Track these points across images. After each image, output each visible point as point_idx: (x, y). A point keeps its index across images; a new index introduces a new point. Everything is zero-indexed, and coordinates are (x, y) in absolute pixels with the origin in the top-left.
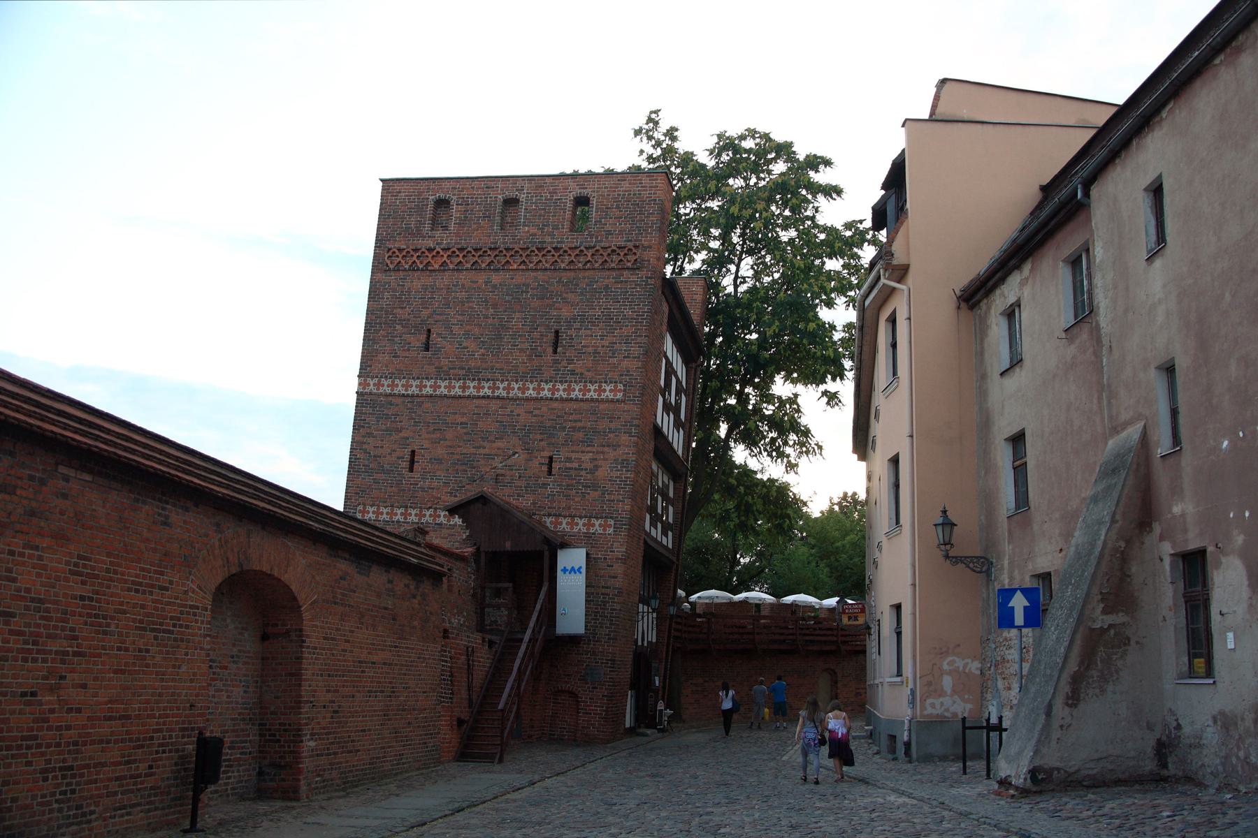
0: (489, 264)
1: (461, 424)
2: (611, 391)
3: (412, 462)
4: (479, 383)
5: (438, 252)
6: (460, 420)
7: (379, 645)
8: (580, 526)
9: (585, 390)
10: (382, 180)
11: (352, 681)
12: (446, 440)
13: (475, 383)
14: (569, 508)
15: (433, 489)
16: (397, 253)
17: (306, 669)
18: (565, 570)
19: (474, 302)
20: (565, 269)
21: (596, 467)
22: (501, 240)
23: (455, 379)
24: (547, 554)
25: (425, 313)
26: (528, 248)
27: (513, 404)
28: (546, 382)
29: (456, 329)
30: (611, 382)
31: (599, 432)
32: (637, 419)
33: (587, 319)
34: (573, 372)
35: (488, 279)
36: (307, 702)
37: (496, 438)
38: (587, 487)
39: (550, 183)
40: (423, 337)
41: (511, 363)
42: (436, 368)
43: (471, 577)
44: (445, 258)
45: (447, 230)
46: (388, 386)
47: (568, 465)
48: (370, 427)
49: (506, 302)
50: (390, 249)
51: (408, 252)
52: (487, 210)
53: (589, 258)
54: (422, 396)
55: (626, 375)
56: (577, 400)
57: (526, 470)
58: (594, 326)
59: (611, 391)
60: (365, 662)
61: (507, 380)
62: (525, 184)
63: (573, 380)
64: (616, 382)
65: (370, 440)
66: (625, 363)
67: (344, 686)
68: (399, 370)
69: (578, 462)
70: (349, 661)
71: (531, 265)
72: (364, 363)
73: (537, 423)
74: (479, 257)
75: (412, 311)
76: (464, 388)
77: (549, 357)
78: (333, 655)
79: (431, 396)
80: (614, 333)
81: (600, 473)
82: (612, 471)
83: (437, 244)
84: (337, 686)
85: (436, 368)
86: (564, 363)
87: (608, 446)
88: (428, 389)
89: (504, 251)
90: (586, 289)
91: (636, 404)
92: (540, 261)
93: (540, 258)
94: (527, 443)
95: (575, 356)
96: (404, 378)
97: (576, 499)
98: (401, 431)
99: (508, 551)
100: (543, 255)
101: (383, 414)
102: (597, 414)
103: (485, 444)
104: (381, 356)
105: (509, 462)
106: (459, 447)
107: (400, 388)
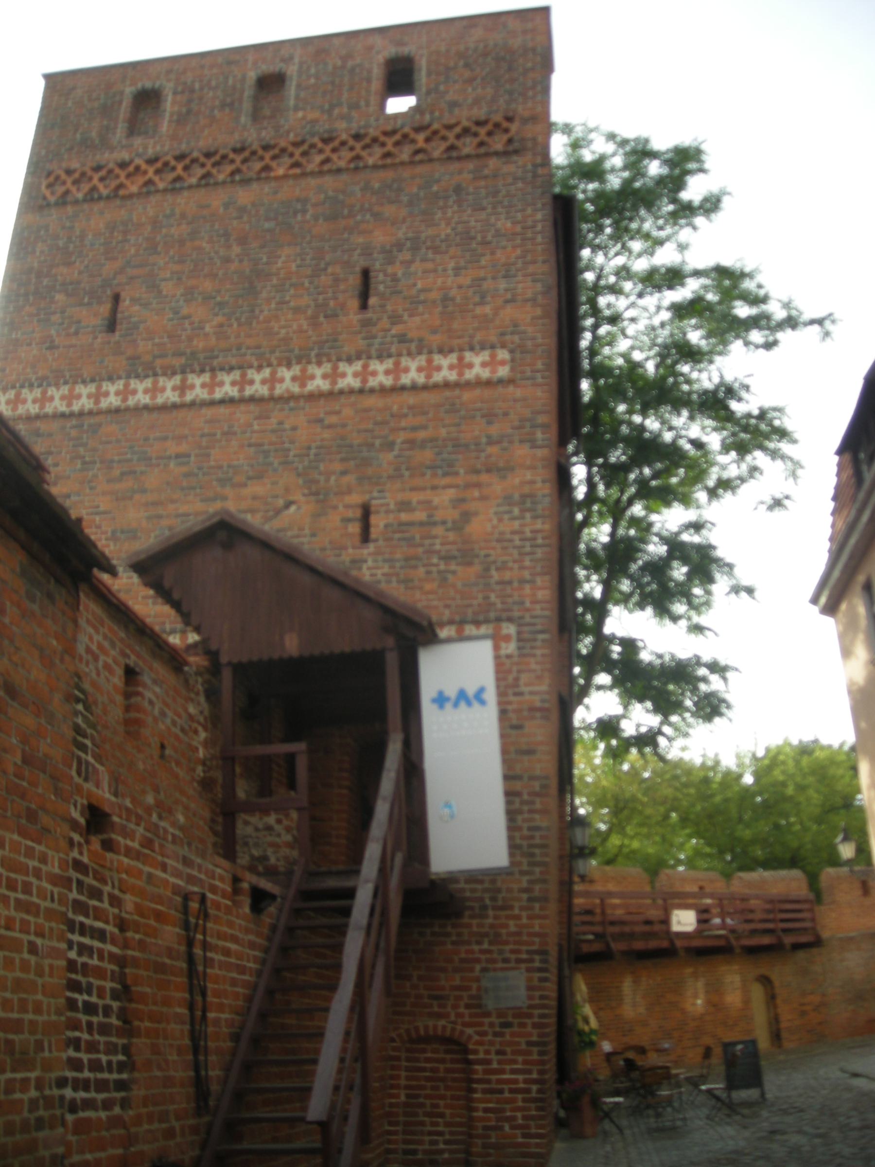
0: (233, 174)
1: (178, 456)
4: (213, 377)
6: (172, 448)
9: (430, 368)
13: (206, 377)
21: (467, 516)
22: (253, 136)
23: (164, 374)
24: (392, 661)
26: (303, 142)
27: (282, 410)
28: (349, 360)
29: (167, 288)
30: (483, 348)
31: (466, 446)
33: (424, 243)
34: (402, 339)
37: (249, 478)
38: (447, 558)
40: (105, 309)
42: (128, 359)
43: (196, 732)
47: (404, 517)
54: (100, 412)
55: (512, 333)
56: (414, 388)
57: (313, 535)
61: (269, 365)
64: (493, 347)
66: (509, 312)
75: (87, 267)
76: (183, 388)
77: (354, 317)
79: (117, 411)
80: (478, 261)
81: (476, 527)
82: (500, 520)
85: (128, 359)
86: (385, 322)
87: (489, 471)
95: (404, 310)
96: (66, 383)
97: (428, 587)
100: (334, 150)
103: (228, 491)
106: (173, 501)
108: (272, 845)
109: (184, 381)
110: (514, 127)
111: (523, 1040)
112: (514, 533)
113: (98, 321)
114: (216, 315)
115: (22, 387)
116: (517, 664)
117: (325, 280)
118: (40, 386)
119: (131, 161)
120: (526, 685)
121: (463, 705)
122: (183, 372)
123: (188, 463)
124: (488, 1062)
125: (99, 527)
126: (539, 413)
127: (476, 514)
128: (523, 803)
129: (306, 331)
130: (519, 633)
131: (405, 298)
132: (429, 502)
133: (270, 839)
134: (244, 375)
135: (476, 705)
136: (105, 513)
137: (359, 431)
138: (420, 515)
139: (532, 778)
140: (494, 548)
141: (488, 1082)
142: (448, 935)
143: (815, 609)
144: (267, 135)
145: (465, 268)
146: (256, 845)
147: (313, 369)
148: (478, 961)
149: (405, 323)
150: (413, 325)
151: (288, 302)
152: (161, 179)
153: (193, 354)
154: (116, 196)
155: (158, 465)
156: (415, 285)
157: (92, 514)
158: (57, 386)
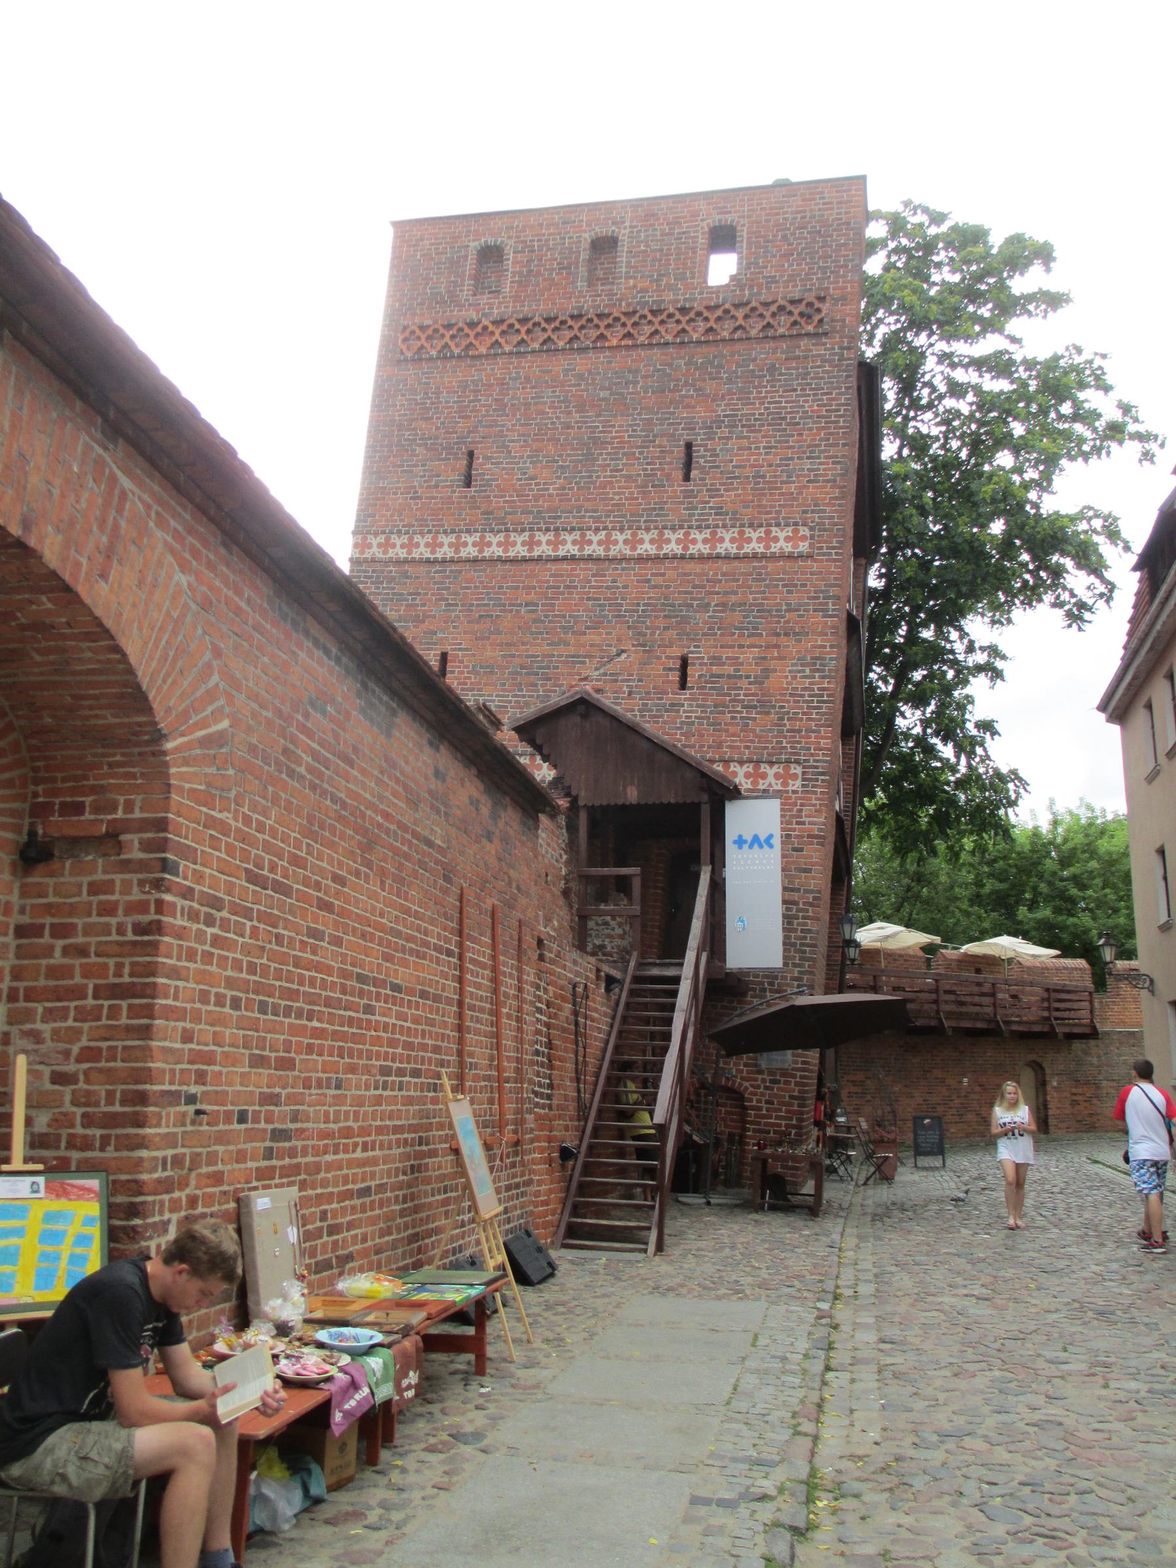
0: (571, 341)
4: (557, 535)
5: (485, 328)
7: (409, 939)
9: (742, 540)
11: (336, 1036)
12: (499, 633)
13: (550, 536)
14: (720, 746)
16: (418, 332)
17: (175, 973)
18: (740, 842)
20: (699, 342)
22: (589, 304)
23: (515, 531)
24: (706, 810)
26: (635, 312)
27: (616, 569)
28: (673, 529)
30: (787, 525)
31: (769, 611)
32: (835, 585)
33: (740, 421)
36: (173, 1098)
37: (587, 628)
41: (612, 499)
44: (497, 336)
46: (403, 546)
49: (600, 400)
50: (405, 328)
52: (566, 258)
53: (740, 322)
54: (460, 561)
55: (813, 512)
56: (727, 557)
59: (787, 539)
60: (377, 983)
63: (720, 523)
64: (796, 524)
67: (310, 1049)
68: (423, 520)
70: (329, 970)
75: (443, 423)
77: (679, 487)
78: (279, 939)
79: (475, 561)
80: (787, 442)
81: (771, 683)
82: (794, 678)
84: (288, 1046)
85: (483, 514)
90: (735, 372)
92: (656, 332)
94: (640, 634)
96: (429, 532)
97: (732, 729)
98: (423, 622)
99: (631, 805)
100: (662, 322)
101: (394, 594)
102: (765, 580)
106: (523, 644)
107: (422, 549)
110: (825, 308)
111: (787, 1095)
112: (804, 689)
113: (457, 477)
114: (559, 478)
119: (479, 322)
120: (807, 816)
121: (756, 846)
122: (531, 529)
123: (536, 611)
125: (461, 662)
126: (832, 586)
127: (775, 671)
128: (799, 910)
129: (637, 499)
130: (804, 773)
132: (738, 658)
133: (607, 931)
135: (765, 847)
136: (466, 649)
137: (680, 593)
138: (729, 670)
139: (806, 891)
140: (788, 702)
142: (736, 1009)
143: (1102, 716)
144: (602, 303)
145: (776, 447)
146: (597, 936)
147: (642, 535)
149: (722, 496)
153: (539, 512)
154: (467, 356)
157: (455, 650)
158: (422, 534)
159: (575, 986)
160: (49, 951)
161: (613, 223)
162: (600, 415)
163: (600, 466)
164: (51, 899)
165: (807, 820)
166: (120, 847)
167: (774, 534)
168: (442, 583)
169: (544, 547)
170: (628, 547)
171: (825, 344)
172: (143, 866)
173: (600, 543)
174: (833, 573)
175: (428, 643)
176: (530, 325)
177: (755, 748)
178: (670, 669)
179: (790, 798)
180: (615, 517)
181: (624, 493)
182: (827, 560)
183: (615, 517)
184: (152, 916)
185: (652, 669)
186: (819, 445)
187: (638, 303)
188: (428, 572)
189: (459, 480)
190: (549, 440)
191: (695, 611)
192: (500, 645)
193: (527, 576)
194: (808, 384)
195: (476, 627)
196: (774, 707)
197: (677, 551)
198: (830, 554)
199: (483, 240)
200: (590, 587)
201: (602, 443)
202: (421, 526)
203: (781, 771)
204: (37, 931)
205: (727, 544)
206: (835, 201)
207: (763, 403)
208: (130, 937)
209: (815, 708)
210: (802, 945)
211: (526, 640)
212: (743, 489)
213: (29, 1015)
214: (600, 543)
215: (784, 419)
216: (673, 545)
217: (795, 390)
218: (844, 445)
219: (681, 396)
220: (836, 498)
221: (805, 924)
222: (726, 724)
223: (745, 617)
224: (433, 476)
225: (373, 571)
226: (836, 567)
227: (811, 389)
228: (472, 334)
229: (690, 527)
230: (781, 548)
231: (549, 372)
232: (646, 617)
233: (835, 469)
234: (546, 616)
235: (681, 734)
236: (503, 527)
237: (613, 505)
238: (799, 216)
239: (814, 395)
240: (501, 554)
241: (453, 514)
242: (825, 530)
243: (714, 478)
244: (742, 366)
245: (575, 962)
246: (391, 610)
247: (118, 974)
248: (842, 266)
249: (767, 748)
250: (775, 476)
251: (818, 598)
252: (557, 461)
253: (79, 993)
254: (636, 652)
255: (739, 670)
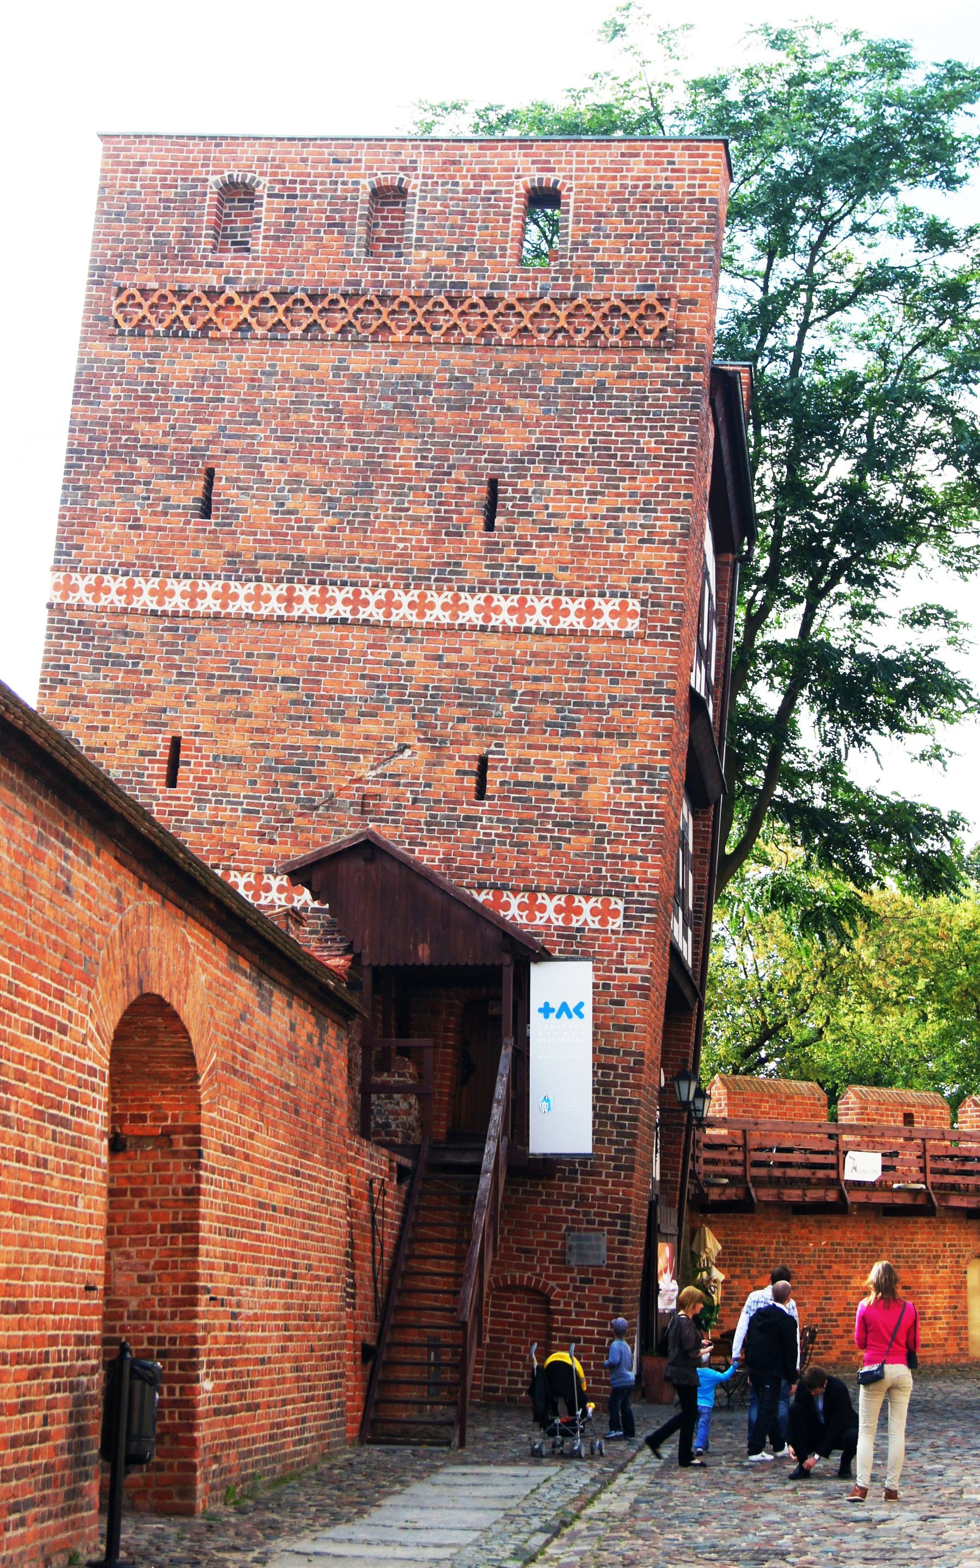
0: (343, 330)
1: (285, 680)
2: (613, 614)
3: (174, 764)
4: (324, 591)
5: (230, 300)
6: (279, 669)
8: (550, 913)
10: (103, 137)
14: (525, 872)
15: (222, 824)
16: (139, 299)
19: (310, 411)
20: (509, 345)
21: (584, 782)
23: (269, 580)
24: (508, 975)
25: (201, 433)
26: (428, 297)
27: (398, 639)
29: (269, 470)
30: (613, 595)
31: (589, 705)
33: (559, 455)
34: (530, 572)
35: (340, 361)
37: (362, 714)
38: (562, 825)
39: (473, 156)
40: (198, 486)
41: (395, 547)
42: (227, 555)
44: (245, 314)
45: (248, 250)
47: (521, 776)
48: (78, 684)
49: (379, 413)
50: (121, 290)
51: (163, 297)
53: (563, 323)
54: (196, 616)
55: (646, 580)
57: (429, 785)
58: (575, 470)
59: (613, 614)
61: (386, 586)
62: (419, 155)
63: (531, 588)
64: (624, 595)
65: (79, 712)
66: (644, 556)
68: (146, 558)
69: (544, 770)
71: (435, 334)
72: (66, 539)
73: (453, 681)
74: (321, 311)
75: (173, 427)
77: (477, 538)
79: (217, 616)
80: (617, 487)
81: (592, 795)
82: (617, 790)
83: (227, 281)
85: (227, 555)
86: (511, 551)
87: (609, 735)
88: (209, 601)
89: (376, 302)
90: (555, 390)
91: (670, 645)
92: (455, 326)
93: (454, 319)
95: (533, 537)
96: (156, 575)
97: (541, 852)
98: (149, 695)
100: (463, 313)
101: (108, 655)
102: (584, 664)
104: (101, 527)
105: (388, 768)
106: (280, 731)
107: (146, 597)
108: (393, 1112)
109: (291, 590)
112: (629, 805)
114: (326, 514)
115: (104, 572)
116: (622, 940)
117: (448, 488)
118: (126, 574)
122: (290, 581)
124: (569, 1313)
125: (199, 750)
127: (594, 781)
129: (427, 549)
130: (626, 909)
131: (534, 521)
132: (549, 763)
133: (390, 1107)
134: (357, 593)
136: (205, 734)
137: (478, 675)
138: (538, 777)
140: (609, 820)
141: (567, 1330)
142: (540, 1194)
145: (602, 494)
146: (379, 1112)
147: (432, 596)
148: (565, 1220)
149: (534, 552)
150: (542, 559)
151: (407, 510)
152: (260, 323)
153: (300, 558)
155: (264, 687)
156: (547, 507)
159: (371, 1181)
160: (131, 1204)
161: (402, 169)
162: (380, 434)
163: (380, 501)
164: (130, 1173)
165: (629, 967)
166: (171, 1143)
167: (596, 607)
168: (173, 644)
169: (306, 605)
170: (415, 612)
171: (668, 361)
172: (187, 1154)
173: (379, 605)
174: (667, 660)
175: (155, 724)
176: (289, 303)
177: (568, 876)
178: (465, 773)
179: (609, 939)
180: (398, 570)
181: (410, 540)
182: (661, 644)
183: (398, 570)
184: (193, 1184)
185: (443, 771)
186: (656, 495)
187: (432, 285)
188: (155, 629)
189: (195, 508)
190: (313, 461)
191: (497, 700)
192: (251, 731)
193: (285, 642)
194: (648, 413)
195: (218, 706)
196: (592, 826)
197: (475, 622)
198: (665, 636)
199: (226, 174)
200: (366, 662)
201: (383, 471)
202: (143, 566)
203: (599, 905)
204: (123, 1192)
205: (538, 616)
206: (687, 167)
207: (588, 434)
208: (181, 1196)
209: (642, 829)
210: (620, 1118)
211: (283, 726)
212: (560, 545)
213: (121, 1243)
214: (379, 605)
215: (615, 456)
216: (471, 614)
217: (629, 420)
218: (686, 496)
219: (485, 416)
220: (674, 565)
221: (626, 1093)
222: (533, 845)
223: (558, 711)
224: (159, 499)
225: (80, 623)
226: (671, 653)
227: (648, 420)
228: (212, 306)
229: (493, 591)
230: (605, 626)
231: (315, 368)
232: (436, 704)
233: (675, 527)
234: (308, 696)
235: (478, 856)
236: (253, 576)
237: (397, 555)
238: (641, 183)
239: (652, 428)
240: (250, 611)
241: (188, 553)
242: (659, 605)
243: (524, 529)
244: (563, 382)
245: (371, 1157)
246: (105, 677)
247: (175, 1218)
248: (692, 259)
249: (582, 877)
250: (600, 532)
251: (649, 691)
252: (324, 492)
253: (152, 1230)
254: (422, 748)
255: (550, 778)
